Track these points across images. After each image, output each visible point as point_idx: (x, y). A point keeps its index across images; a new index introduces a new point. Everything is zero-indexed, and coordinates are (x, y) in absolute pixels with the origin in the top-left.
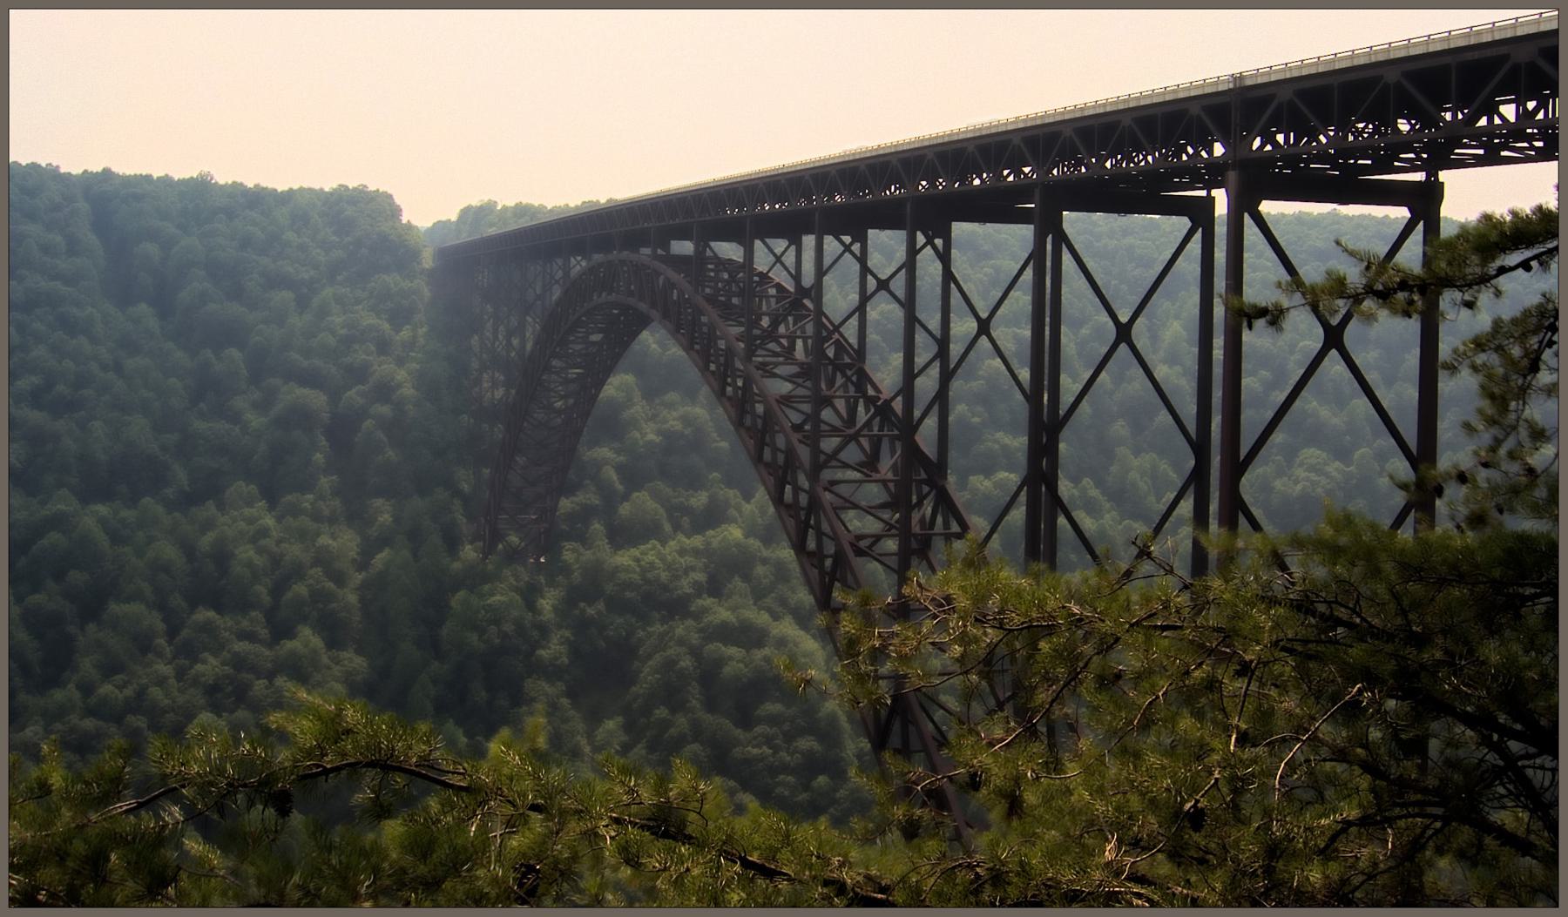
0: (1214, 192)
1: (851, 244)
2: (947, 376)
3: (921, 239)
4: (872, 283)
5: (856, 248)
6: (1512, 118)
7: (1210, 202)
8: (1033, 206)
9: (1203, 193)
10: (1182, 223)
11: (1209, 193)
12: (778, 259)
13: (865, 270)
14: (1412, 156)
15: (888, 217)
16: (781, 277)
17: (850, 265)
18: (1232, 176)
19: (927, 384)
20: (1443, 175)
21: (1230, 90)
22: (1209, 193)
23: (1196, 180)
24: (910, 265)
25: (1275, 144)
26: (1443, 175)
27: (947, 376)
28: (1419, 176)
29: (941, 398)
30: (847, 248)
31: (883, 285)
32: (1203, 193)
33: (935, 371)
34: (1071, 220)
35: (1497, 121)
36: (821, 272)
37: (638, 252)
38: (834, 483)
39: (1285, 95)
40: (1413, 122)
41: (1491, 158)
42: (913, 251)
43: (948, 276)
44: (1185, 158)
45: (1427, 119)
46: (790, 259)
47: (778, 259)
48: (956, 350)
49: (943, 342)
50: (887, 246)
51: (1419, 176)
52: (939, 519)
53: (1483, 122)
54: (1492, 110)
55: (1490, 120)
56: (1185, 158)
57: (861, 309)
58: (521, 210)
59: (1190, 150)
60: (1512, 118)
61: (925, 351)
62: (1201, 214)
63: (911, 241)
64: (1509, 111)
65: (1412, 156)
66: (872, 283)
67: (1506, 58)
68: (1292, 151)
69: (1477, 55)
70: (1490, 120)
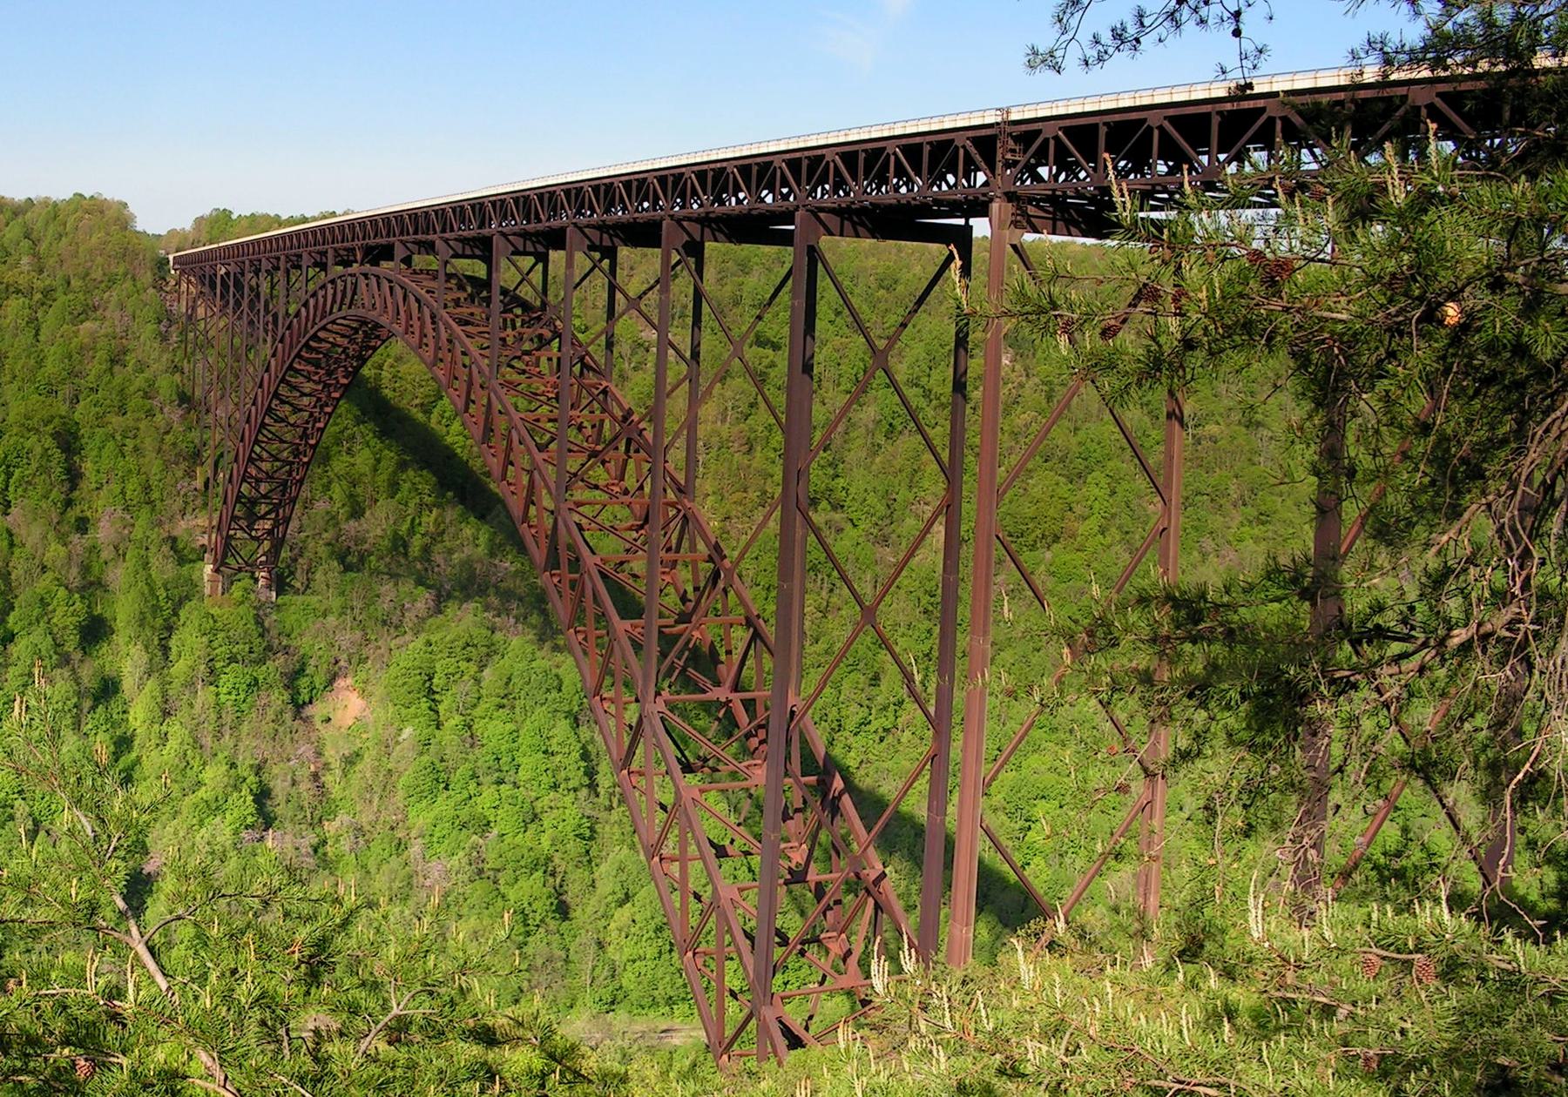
0: (972, 221)
1: (601, 261)
2: (694, 401)
3: (675, 258)
5: (606, 262)
6: (1264, 167)
7: (968, 229)
8: (792, 227)
9: (961, 222)
11: (967, 222)
13: (612, 289)
14: (1166, 196)
15: (645, 235)
16: (526, 292)
17: (599, 281)
19: (678, 404)
21: (998, 124)
22: (967, 222)
23: (955, 209)
24: (662, 282)
25: (1037, 178)
27: (694, 401)
29: (691, 425)
31: (634, 303)
32: (961, 222)
34: (825, 242)
35: (1248, 168)
37: (378, 265)
38: (579, 504)
39: (1049, 131)
40: (1171, 163)
42: (669, 271)
43: (698, 296)
44: (944, 187)
46: (536, 276)
52: (685, 544)
54: (1240, 157)
55: (1241, 168)
56: (944, 187)
58: (254, 221)
59: (951, 179)
60: (1264, 167)
61: (676, 369)
63: (666, 258)
64: (1259, 157)
65: (1166, 196)
68: (1055, 186)
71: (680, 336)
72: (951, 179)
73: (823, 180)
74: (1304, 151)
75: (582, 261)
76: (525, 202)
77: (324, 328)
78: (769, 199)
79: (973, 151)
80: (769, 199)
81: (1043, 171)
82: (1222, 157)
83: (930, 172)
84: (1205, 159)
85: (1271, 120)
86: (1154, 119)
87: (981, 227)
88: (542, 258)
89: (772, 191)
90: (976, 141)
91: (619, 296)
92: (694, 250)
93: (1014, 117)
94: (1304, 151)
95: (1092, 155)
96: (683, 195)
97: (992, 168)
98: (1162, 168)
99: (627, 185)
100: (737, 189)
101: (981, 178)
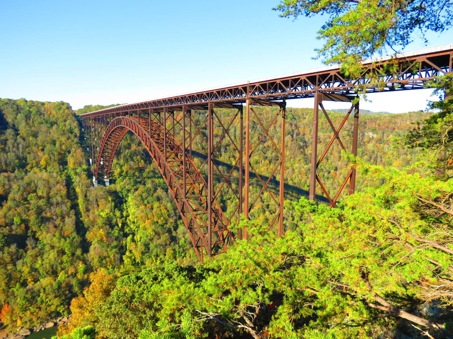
0: (243, 104)
2: (191, 141)
4: (175, 122)
5: (172, 115)
7: (242, 105)
9: (240, 104)
10: (237, 110)
12: (156, 117)
18: (247, 101)
20: (286, 101)
25: (256, 95)
26: (286, 101)
27: (191, 141)
28: (282, 101)
30: (170, 115)
31: (178, 122)
32: (240, 104)
33: (188, 140)
34: (215, 109)
35: (297, 91)
36: (165, 120)
39: (257, 85)
41: (296, 97)
42: (185, 116)
45: (284, 91)
47: (156, 117)
48: (193, 136)
49: (190, 134)
50: (179, 115)
51: (282, 101)
53: (294, 91)
54: (295, 89)
55: (295, 91)
57: (173, 127)
59: (238, 95)
61: (187, 136)
62: (241, 108)
64: (299, 88)
66: (175, 122)
67: (300, 78)
69: (294, 78)
70: (295, 91)
71: (187, 129)
72: (238, 95)
73: (213, 97)
74: (308, 86)
75: (167, 115)
76: (155, 103)
77: (115, 129)
78: (203, 101)
79: (242, 90)
80: (203, 101)
81: (256, 93)
82: (292, 88)
83: (234, 94)
84: (288, 89)
85: (302, 80)
86: (278, 82)
87: (244, 104)
88: (159, 113)
89: (203, 99)
90: (243, 88)
91: (175, 121)
92: (189, 112)
93: (251, 82)
94: (308, 86)
95: (265, 90)
96: (186, 101)
97: (246, 92)
98: (280, 91)
99: (175, 99)
100: (197, 99)
101: (244, 95)
